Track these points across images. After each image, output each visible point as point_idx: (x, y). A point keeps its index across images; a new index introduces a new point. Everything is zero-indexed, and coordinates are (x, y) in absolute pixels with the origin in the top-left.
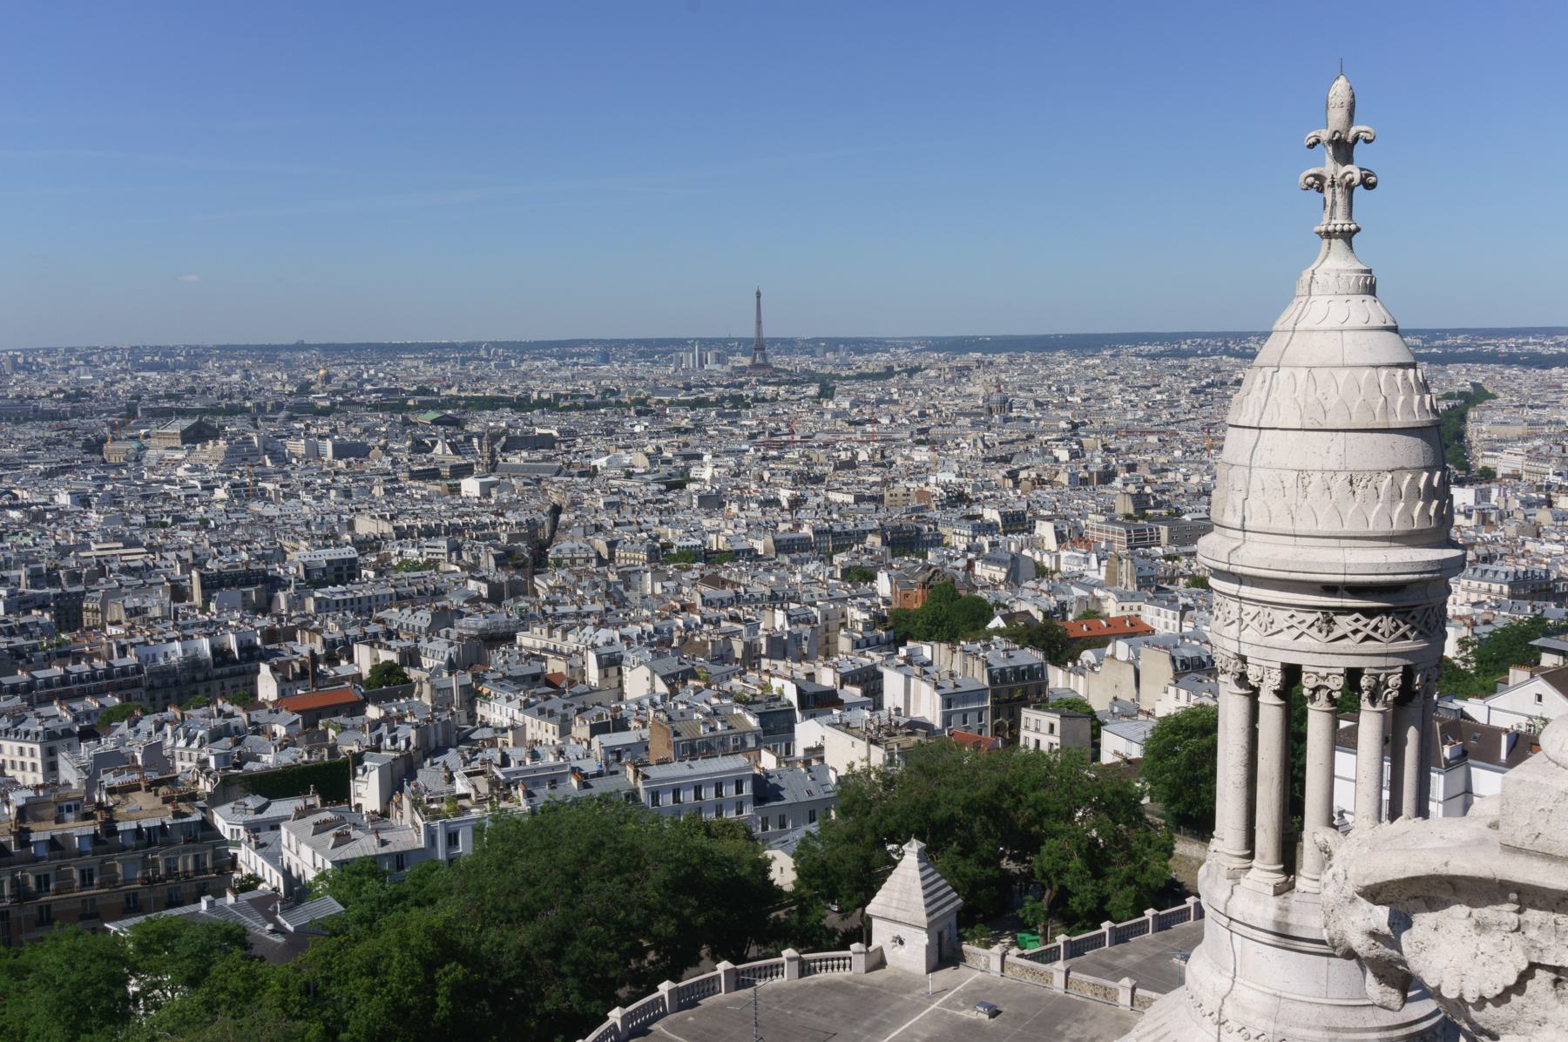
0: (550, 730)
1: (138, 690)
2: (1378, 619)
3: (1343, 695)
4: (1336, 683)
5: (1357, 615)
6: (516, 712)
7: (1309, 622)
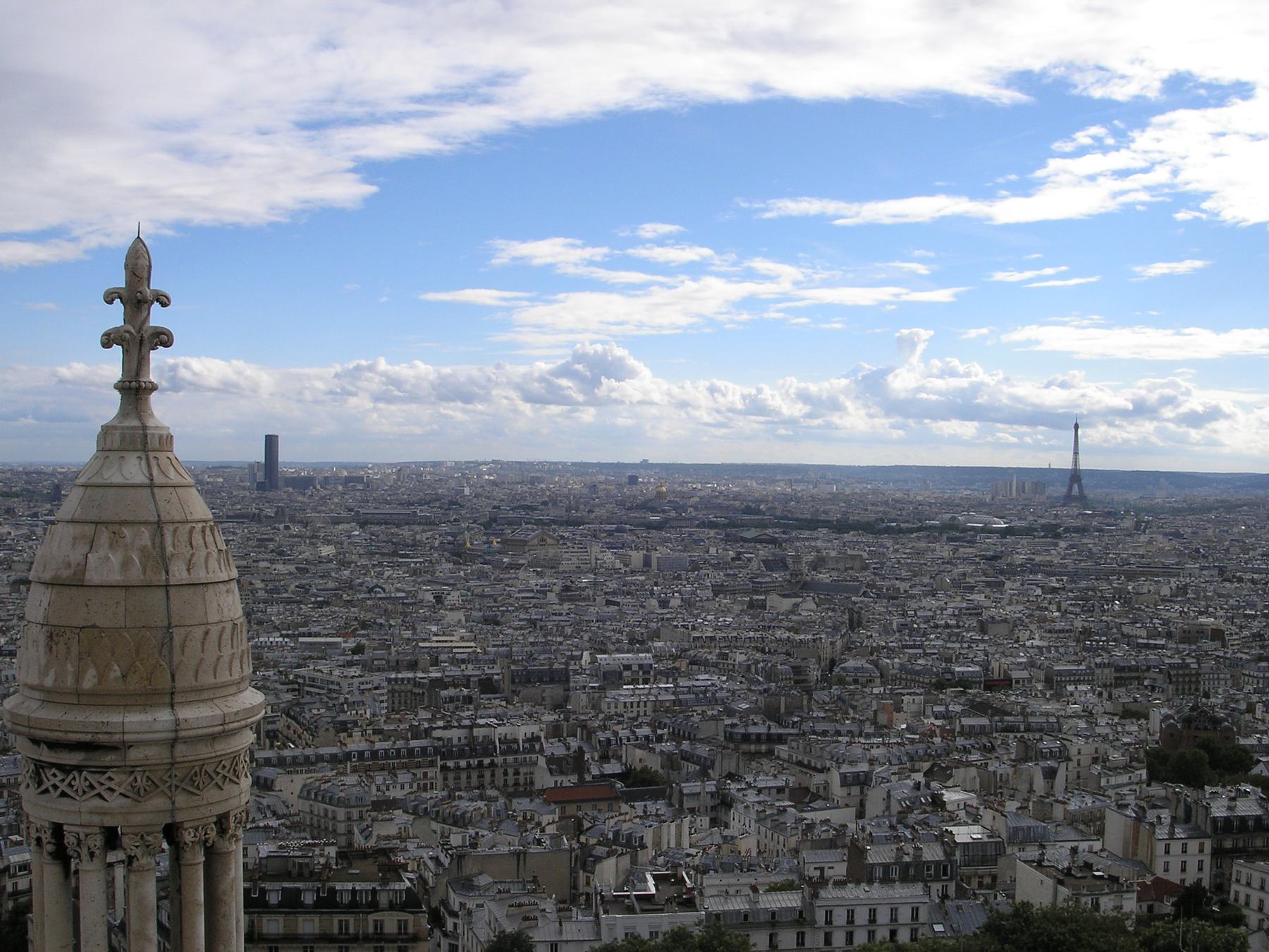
0: (781, 844)
2: (71, 776)
5: (54, 770)
6: (753, 821)
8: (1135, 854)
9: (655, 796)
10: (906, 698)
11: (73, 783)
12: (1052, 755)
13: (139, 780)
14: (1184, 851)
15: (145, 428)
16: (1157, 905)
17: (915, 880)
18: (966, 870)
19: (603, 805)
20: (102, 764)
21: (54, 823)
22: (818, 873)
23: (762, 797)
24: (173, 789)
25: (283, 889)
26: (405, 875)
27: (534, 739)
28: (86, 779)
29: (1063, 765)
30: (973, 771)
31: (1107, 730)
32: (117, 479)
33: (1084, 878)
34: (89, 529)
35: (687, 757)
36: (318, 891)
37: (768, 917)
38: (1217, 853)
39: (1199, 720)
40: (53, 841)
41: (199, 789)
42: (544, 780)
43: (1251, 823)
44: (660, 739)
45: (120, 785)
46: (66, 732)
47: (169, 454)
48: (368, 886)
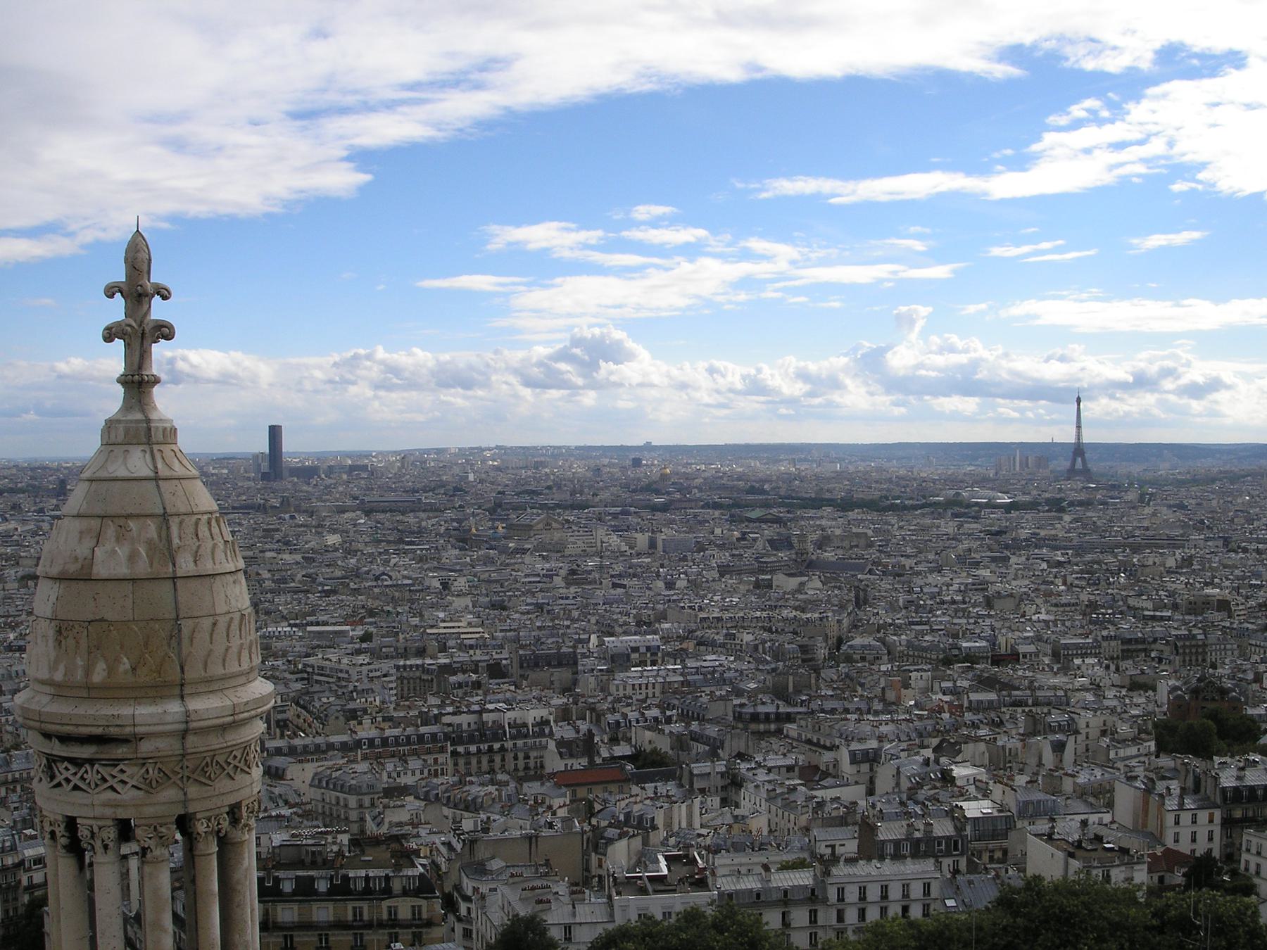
1: (445, 755)
2: (83, 770)
6: (763, 801)
8: (1145, 825)
9: (666, 777)
10: (913, 675)
11: (85, 776)
12: (1061, 729)
13: (151, 771)
14: (1194, 822)
15: (148, 421)
16: (1168, 876)
17: (926, 856)
18: (977, 844)
19: (613, 788)
20: (113, 757)
21: (67, 816)
22: (829, 851)
23: (772, 777)
24: (185, 779)
25: (297, 878)
26: (418, 861)
27: (544, 723)
28: (98, 772)
29: (1072, 738)
30: (982, 746)
31: (1115, 703)
32: (122, 473)
33: (1096, 850)
34: (95, 523)
35: (696, 738)
36: (331, 878)
37: (780, 895)
38: (1228, 823)
39: (1205, 691)
40: (67, 834)
41: (210, 778)
42: (554, 763)
43: (1260, 792)
44: (669, 720)
45: (132, 777)
46: (78, 726)
47: (173, 447)
48: (381, 872)
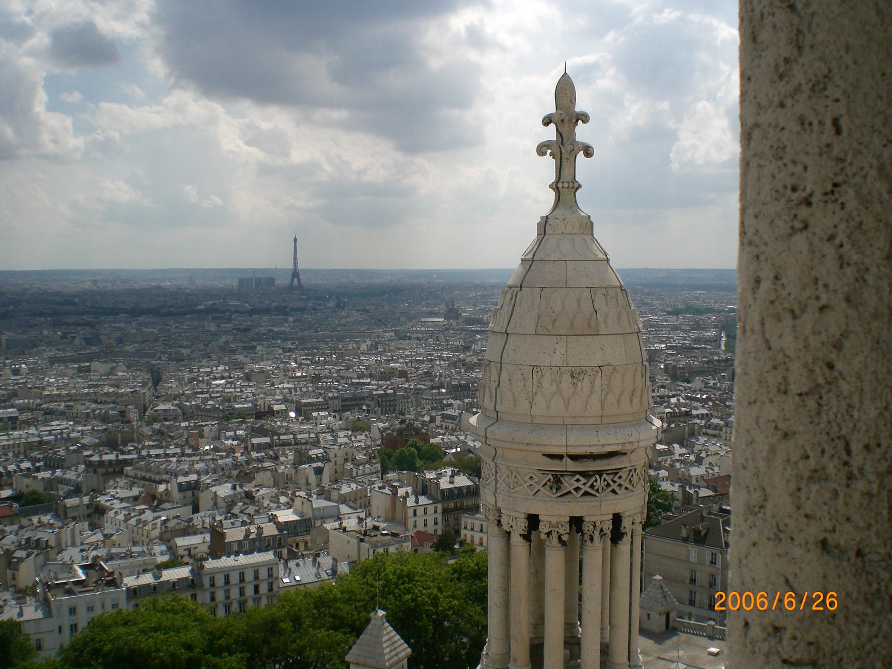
0: (145, 536)
2: (594, 479)
3: (570, 538)
4: (564, 530)
5: (578, 476)
6: (122, 522)
7: (544, 482)
9: (46, 511)
10: (206, 429)
11: (595, 484)
12: (318, 459)
14: (425, 513)
16: (420, 549)
18: (290, 540)
21: (570, 517)
22: (187, 552)
28: (605, 480)
29: (327, 465)
30: (269, 474)
31: (346, 440)
35: (60, 481)
38: (445, 511)
43: (465, 491)
44: (38, 470)
46: (603, 445)
